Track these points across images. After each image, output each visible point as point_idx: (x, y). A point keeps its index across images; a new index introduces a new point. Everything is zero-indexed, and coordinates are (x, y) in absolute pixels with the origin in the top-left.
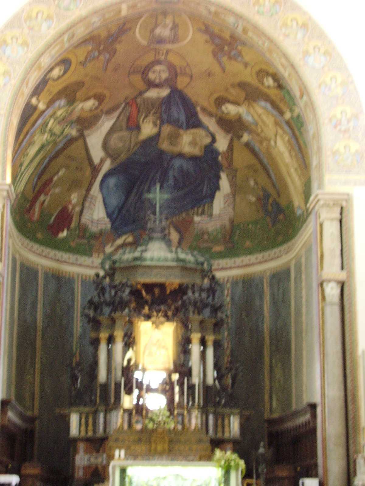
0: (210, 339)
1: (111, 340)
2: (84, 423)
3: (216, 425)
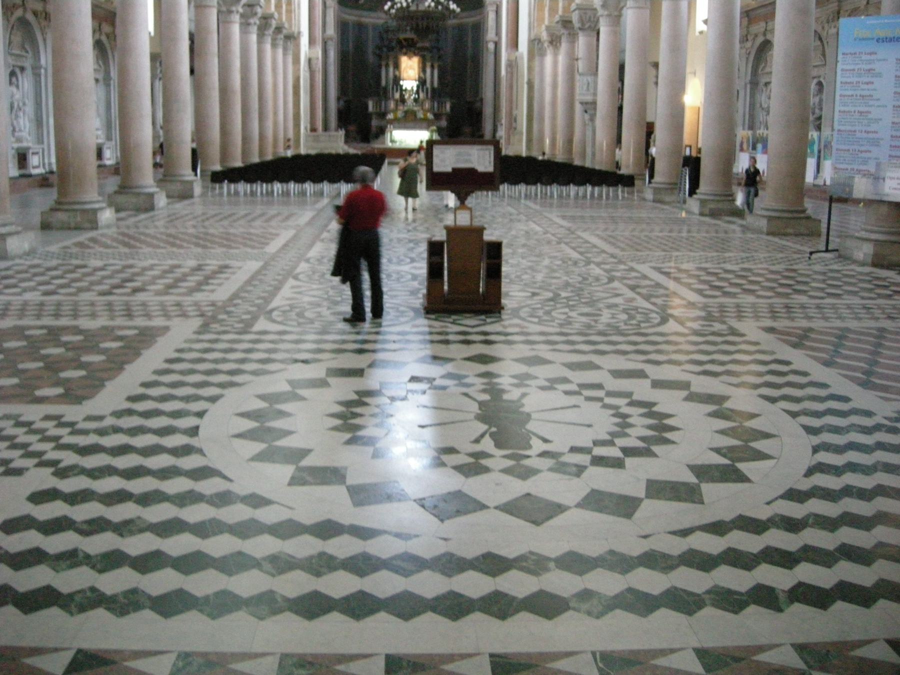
0: (436, 65)
1: (387, 66)
2: (375, 106)
3: (438, 107)
